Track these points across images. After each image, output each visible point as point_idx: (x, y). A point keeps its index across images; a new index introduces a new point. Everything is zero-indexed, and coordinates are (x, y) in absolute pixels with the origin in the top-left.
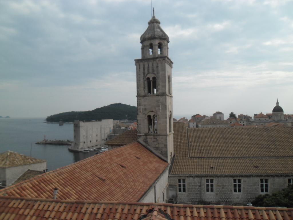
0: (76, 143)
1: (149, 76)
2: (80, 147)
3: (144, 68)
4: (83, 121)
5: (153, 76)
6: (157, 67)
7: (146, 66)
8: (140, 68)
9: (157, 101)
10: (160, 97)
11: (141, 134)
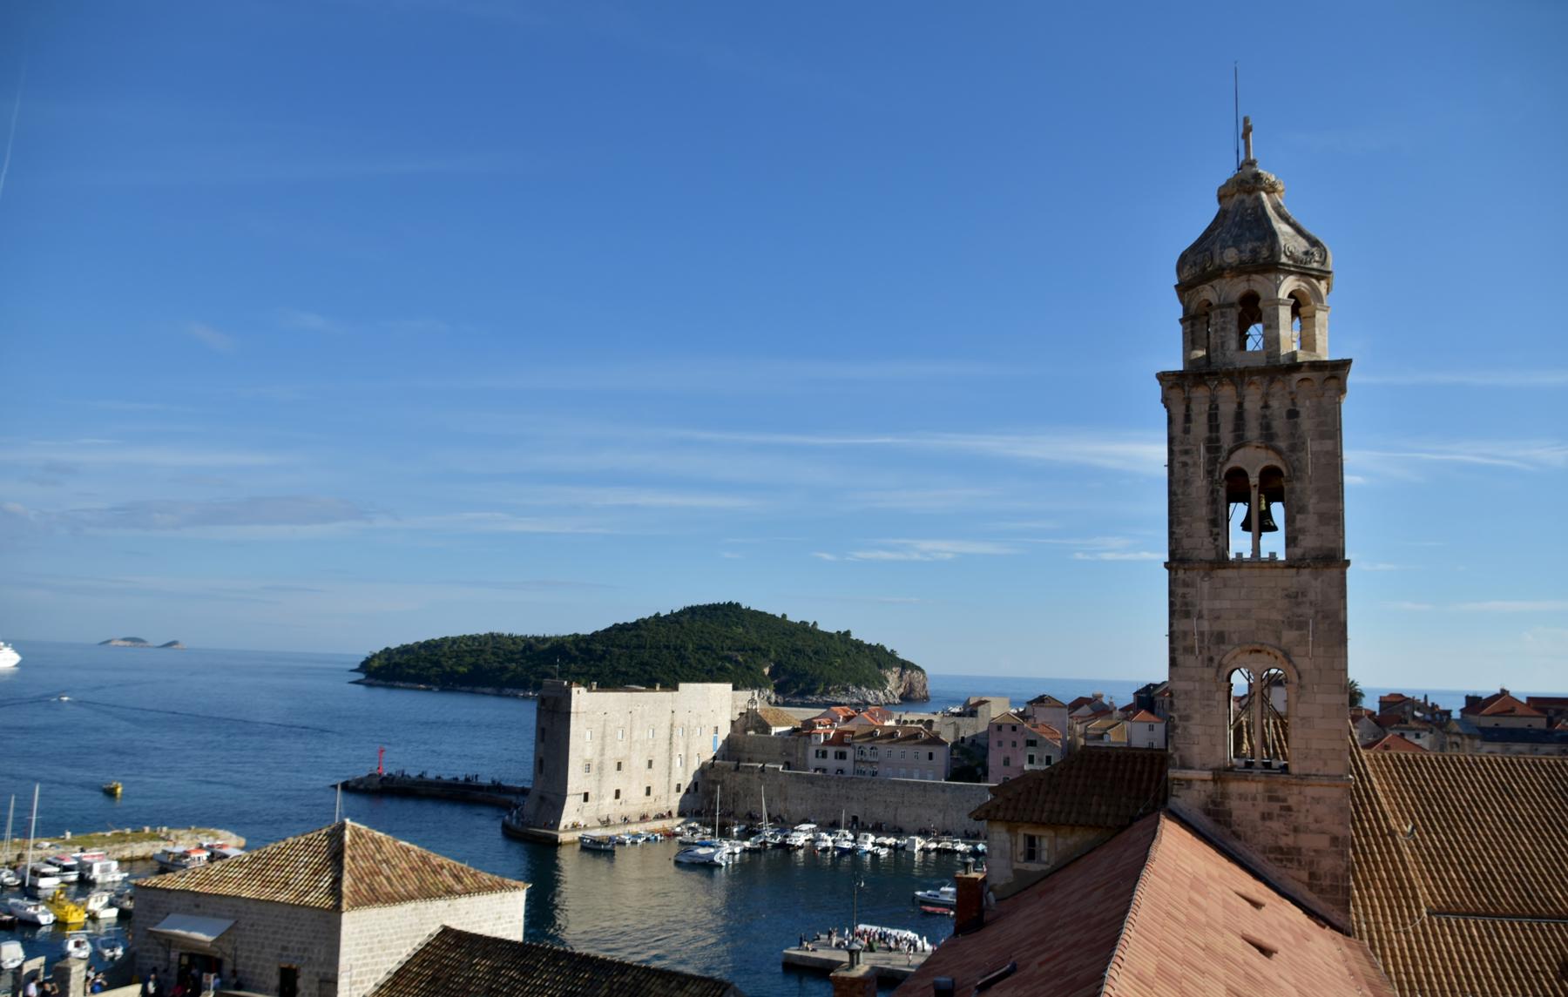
0: (542, 798)
1: (1238, 460)
2: (567, 819)
3: (1213, 418)
4: (590, 690)
5: (1267, 459)
6: (1293, 414)
7: (1227, 409)
8: (1188, 418)
9: (1288, 596)
10: (1306, 574)
11: (1190, 774)
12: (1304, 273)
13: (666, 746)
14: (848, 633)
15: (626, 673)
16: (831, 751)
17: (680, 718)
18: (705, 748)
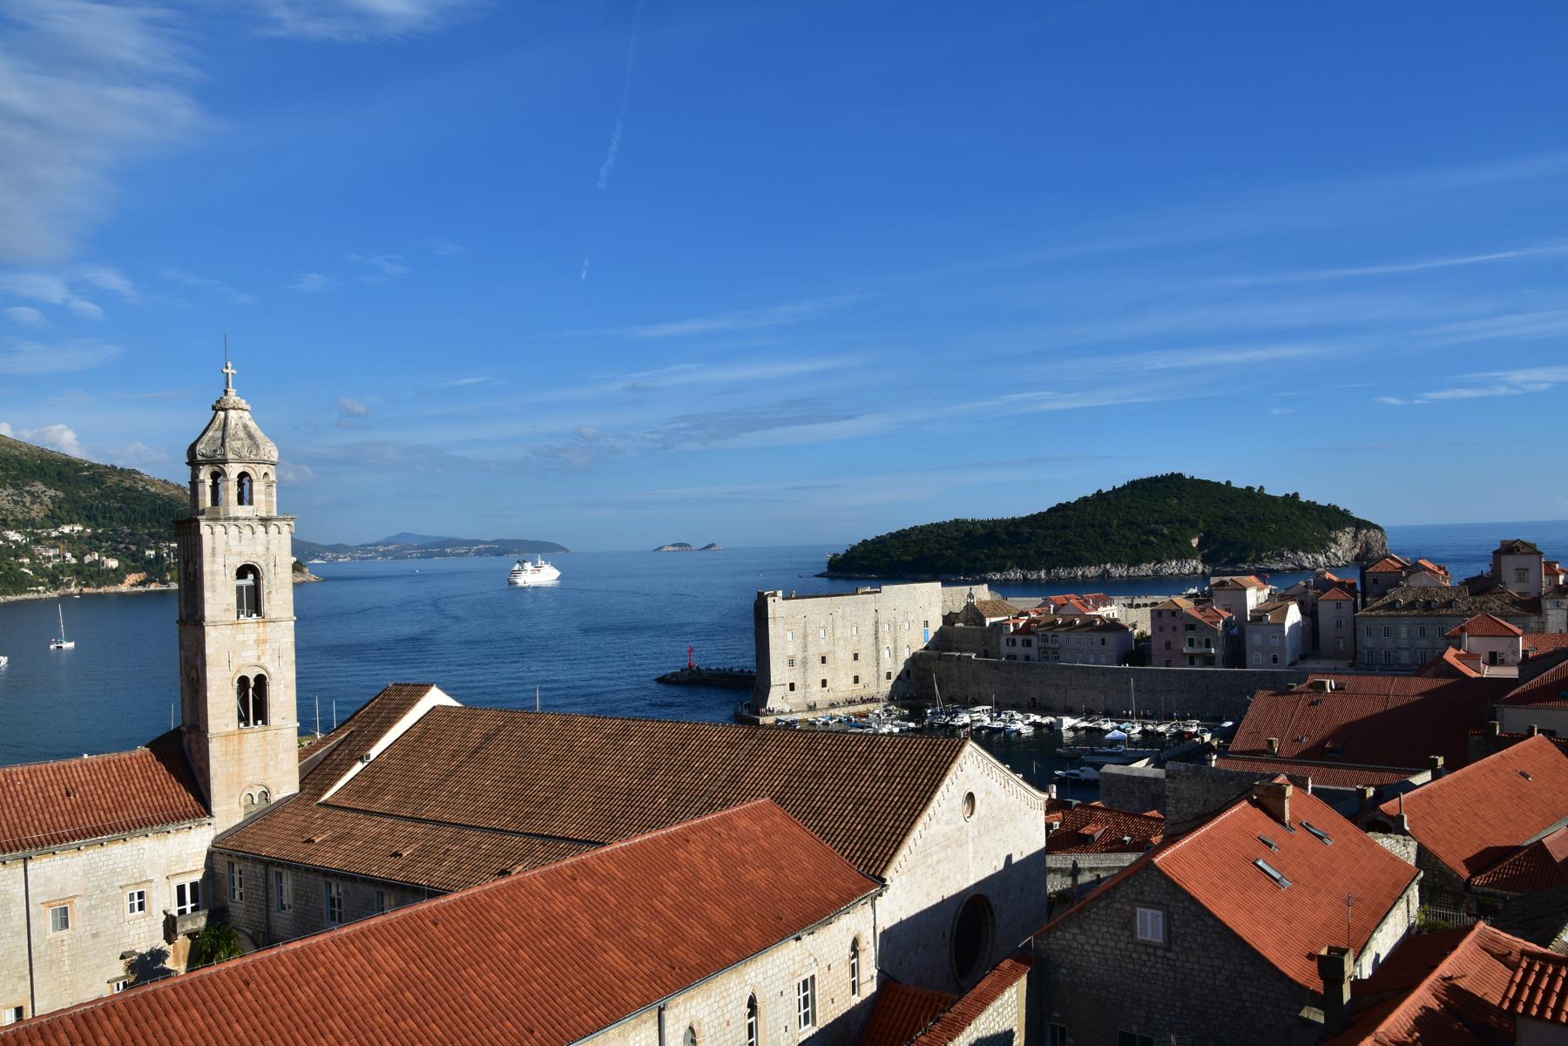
12: (211, 461)
13: (871, 640)
14: (1296, 495)
15: (1050, 554)
16: (1019, 639)
17: (884, 616)
18: (915, 640)
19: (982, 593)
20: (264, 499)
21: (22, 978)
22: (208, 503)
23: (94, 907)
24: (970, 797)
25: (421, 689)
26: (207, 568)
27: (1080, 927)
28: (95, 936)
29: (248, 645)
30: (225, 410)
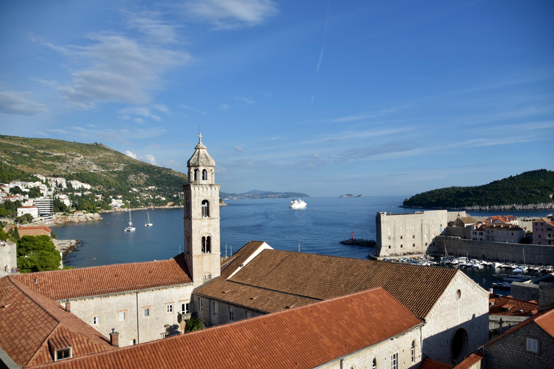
12: (194, 166)
13: (420, 231)
15: (491, 200)
16: (478, 232)
17: (424, 222)
18: (437, 231)
19: (463, 214)
20: (211, 178)
21: (135, 330)
22: (193, 180)
23: (157, 309)
24: (459, 291)
25: (260, 243)
26: (193, 201)
27: (503, 344)
28: (157, 319)
29: (205, 226)
30: (199, 149)
